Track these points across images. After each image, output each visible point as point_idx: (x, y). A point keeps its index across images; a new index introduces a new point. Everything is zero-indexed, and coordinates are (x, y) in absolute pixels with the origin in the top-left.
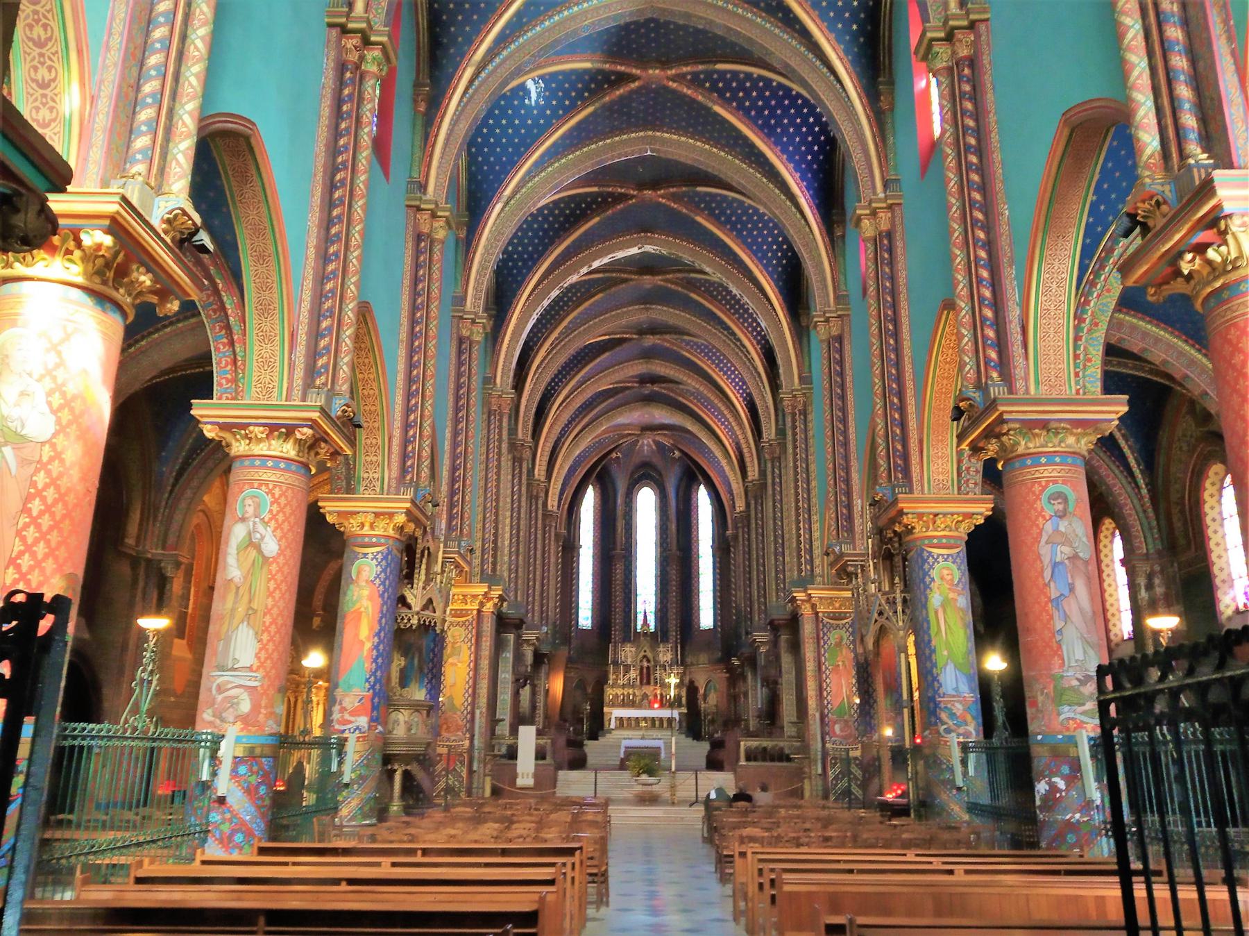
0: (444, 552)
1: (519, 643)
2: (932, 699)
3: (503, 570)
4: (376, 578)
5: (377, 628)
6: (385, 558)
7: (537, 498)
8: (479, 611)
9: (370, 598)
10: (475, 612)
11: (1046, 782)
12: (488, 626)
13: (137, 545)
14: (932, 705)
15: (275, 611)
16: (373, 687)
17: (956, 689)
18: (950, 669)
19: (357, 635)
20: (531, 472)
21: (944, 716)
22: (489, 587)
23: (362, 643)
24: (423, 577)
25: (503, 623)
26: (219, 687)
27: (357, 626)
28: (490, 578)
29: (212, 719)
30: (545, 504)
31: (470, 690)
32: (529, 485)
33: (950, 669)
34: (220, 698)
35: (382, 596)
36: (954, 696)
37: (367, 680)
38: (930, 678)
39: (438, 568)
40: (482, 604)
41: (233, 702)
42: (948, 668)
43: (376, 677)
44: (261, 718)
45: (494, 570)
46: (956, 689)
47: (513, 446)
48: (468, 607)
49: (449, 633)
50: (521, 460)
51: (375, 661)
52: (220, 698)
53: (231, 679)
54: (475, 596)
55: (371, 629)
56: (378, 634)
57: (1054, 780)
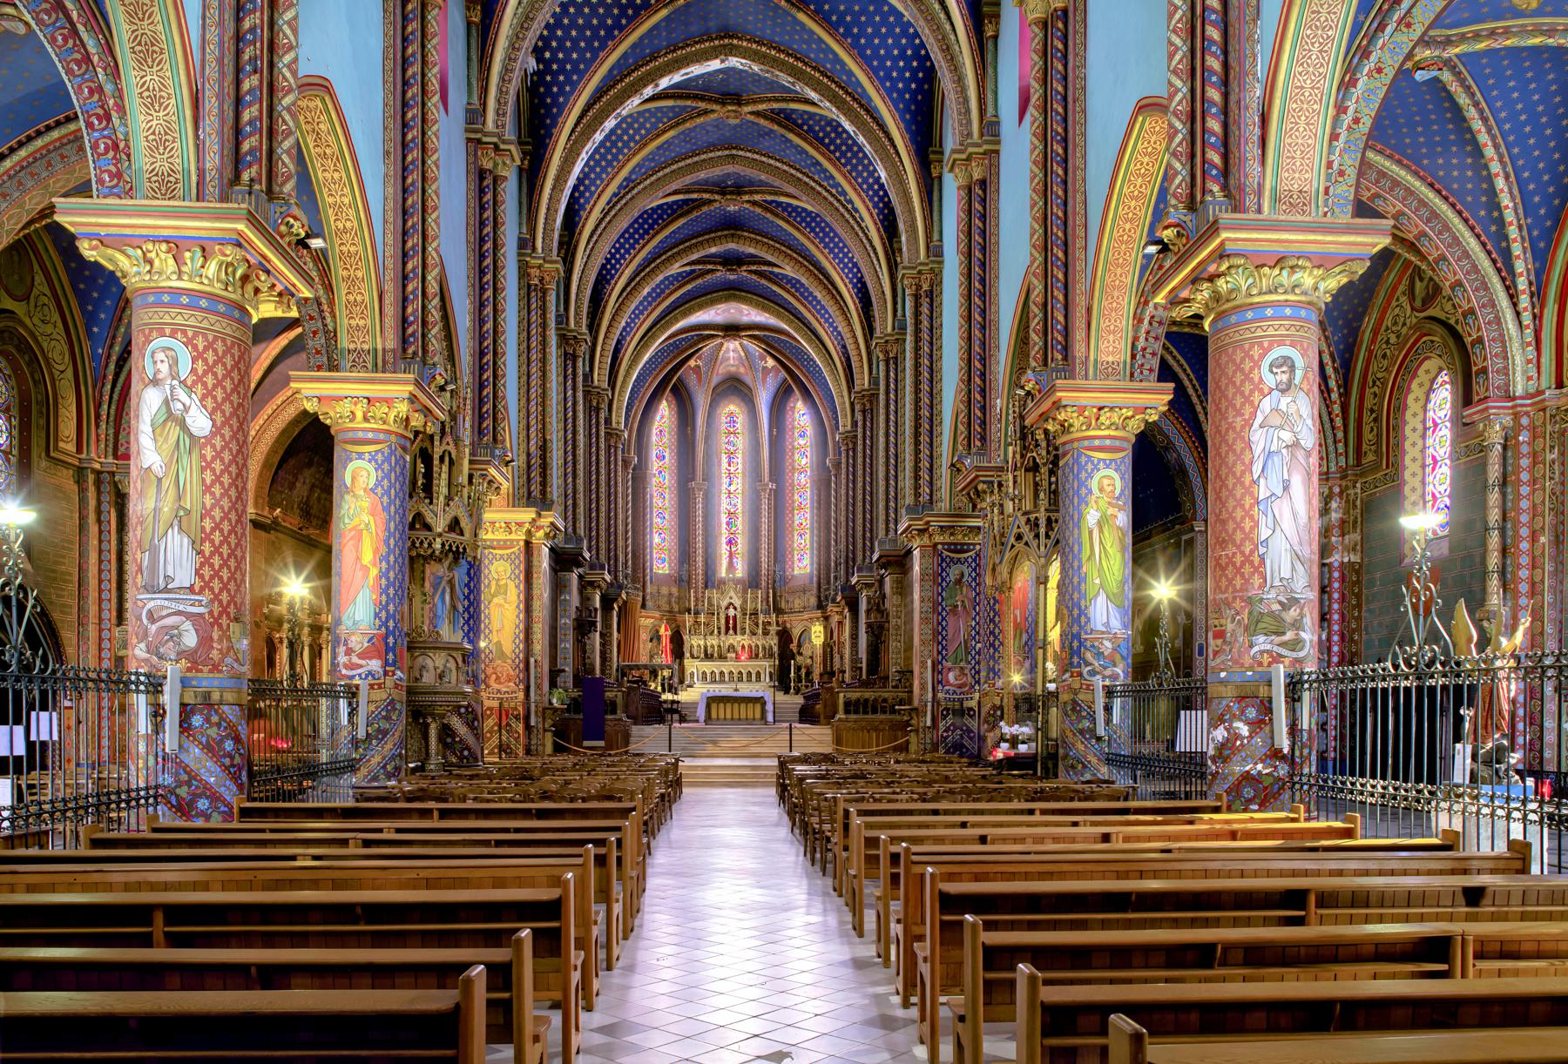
0: (471, 462)
1: (585, 585)
2: (1077, 636)
3: (555, 491)
4: (376, 486)
5: (384, 550)
6: (388, 459)
7: (598, 410)
8: (528, 543)
9: (372, 513)
10: (522, 543)
11: (1225, 728)
12: (544, 562)
13: (79, 450)
14: (1076, 644)
15: (217, 514)
16: (385, 624)
17: (1107, 624)
18: (1101, 600)
19: (358, 559)
20: (588, 377)
21: (1089, 656)
22: (539, 515)
23: (366, 569)
24: (444, 490)
25: (563, 560)
26: (150, 614)
27: (358, 549)
28: (541, 501)
29: (145, 655)
30: (608, 421)
31: (522, 636)
32: (587, 393)
33: (1102, 599)
34: (153, 628)
35: (386, 509)
36: (1103, 633)
37: (377, 615)
38: (1076, 612)
39: (464, 479)
40: (529, 532)
41: (172, 634)
42: (1099, 599)
43: (387, 612)
44: (215, 654)
45: (544, 492)
46: (1107, 624)
47: (563, 339)
48: (513, 537)
49: (492, 568)
50: (574, 357)
51: (385, 591)
52: (153, 628)
53: (166, 603)
54: (520, 524)
55: (376, 552)
56: (386, 558)
57: (1235, 725)
